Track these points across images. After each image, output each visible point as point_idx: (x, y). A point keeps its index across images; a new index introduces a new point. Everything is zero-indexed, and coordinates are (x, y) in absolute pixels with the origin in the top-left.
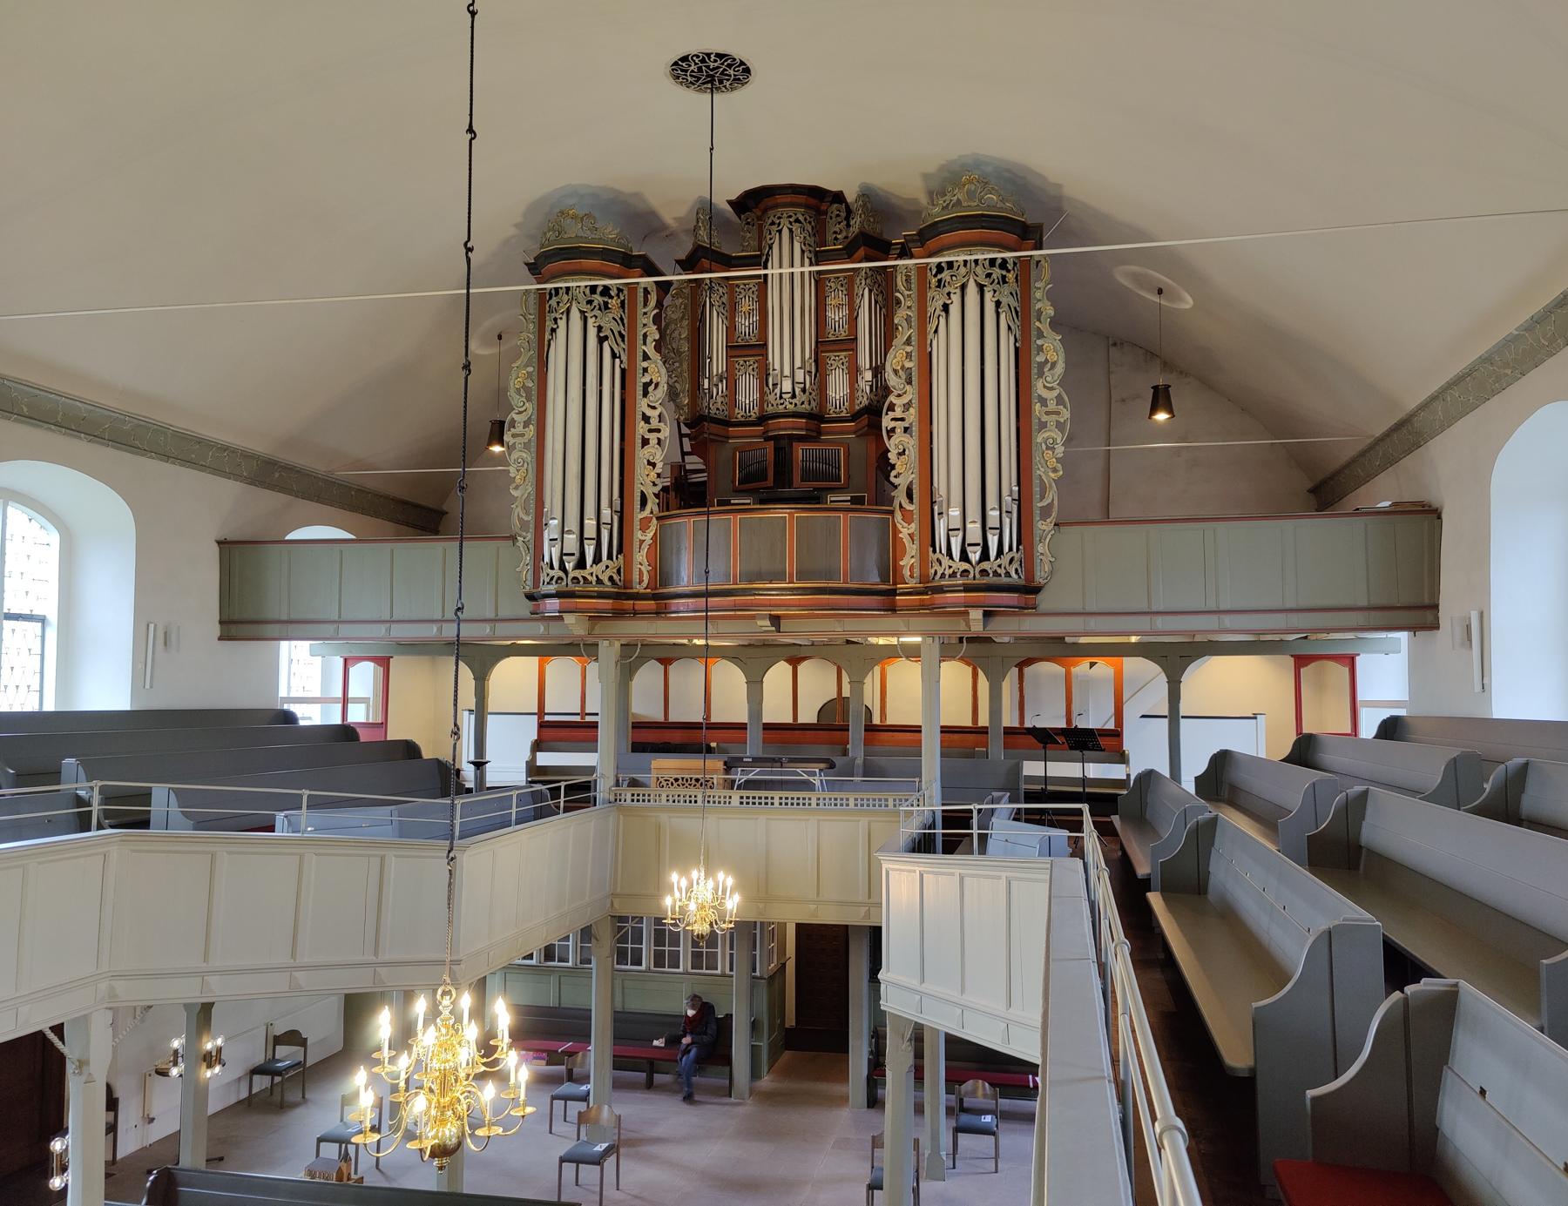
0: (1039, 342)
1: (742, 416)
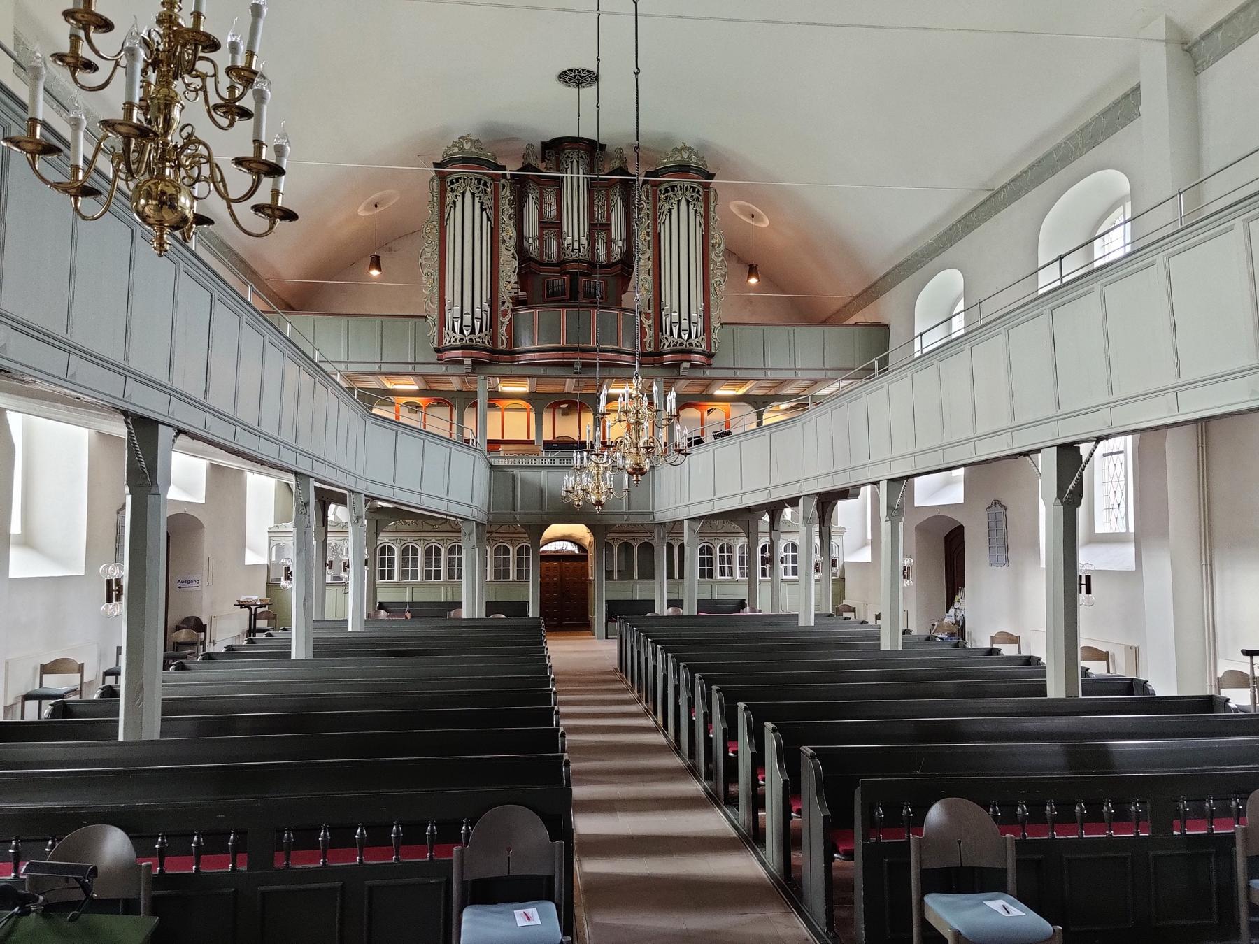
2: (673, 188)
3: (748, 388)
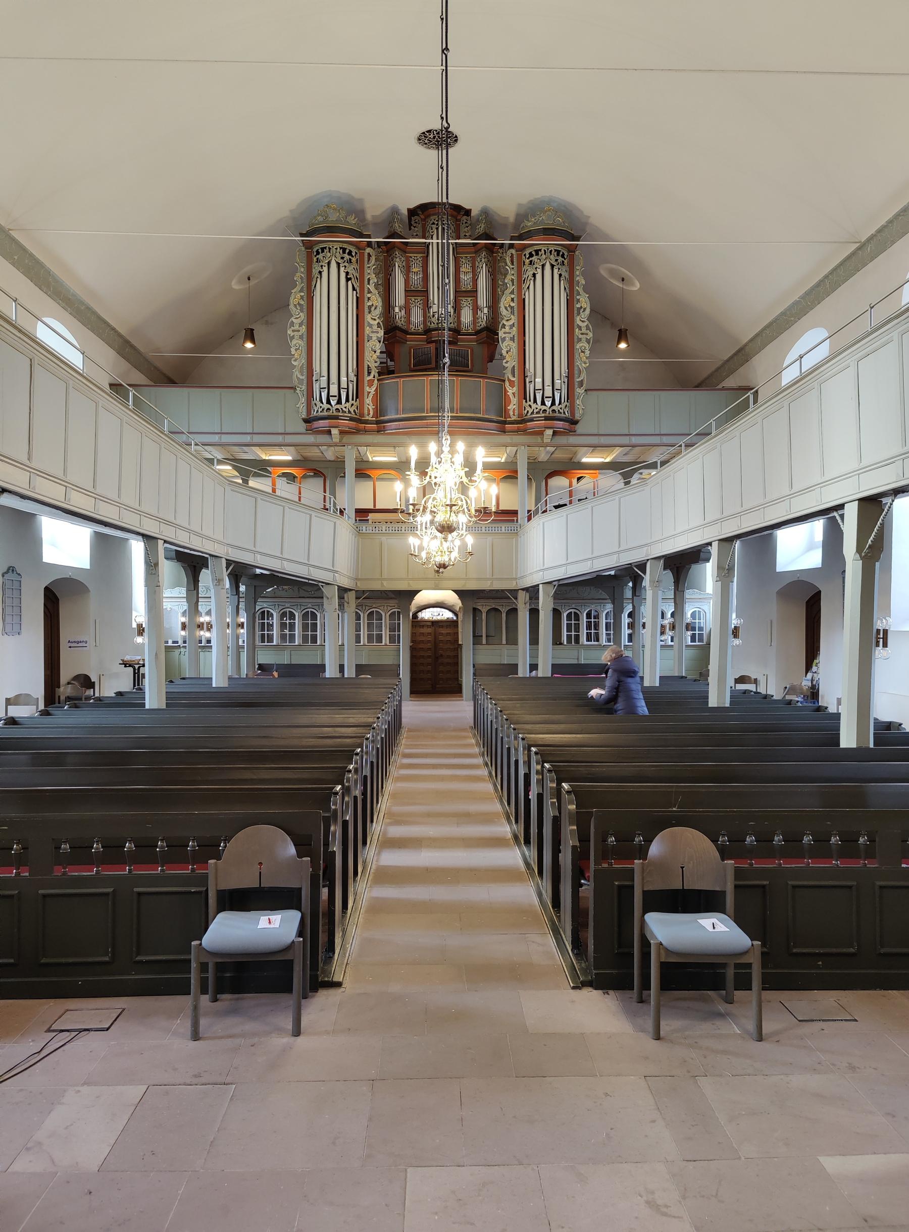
0: (578, 297)
1: (414, 330)
2: (537, 252)
3: (614, 455)
